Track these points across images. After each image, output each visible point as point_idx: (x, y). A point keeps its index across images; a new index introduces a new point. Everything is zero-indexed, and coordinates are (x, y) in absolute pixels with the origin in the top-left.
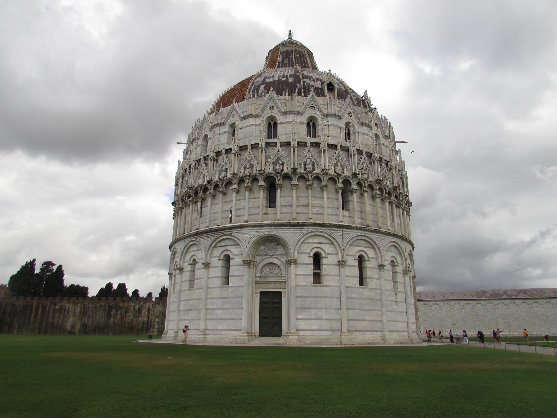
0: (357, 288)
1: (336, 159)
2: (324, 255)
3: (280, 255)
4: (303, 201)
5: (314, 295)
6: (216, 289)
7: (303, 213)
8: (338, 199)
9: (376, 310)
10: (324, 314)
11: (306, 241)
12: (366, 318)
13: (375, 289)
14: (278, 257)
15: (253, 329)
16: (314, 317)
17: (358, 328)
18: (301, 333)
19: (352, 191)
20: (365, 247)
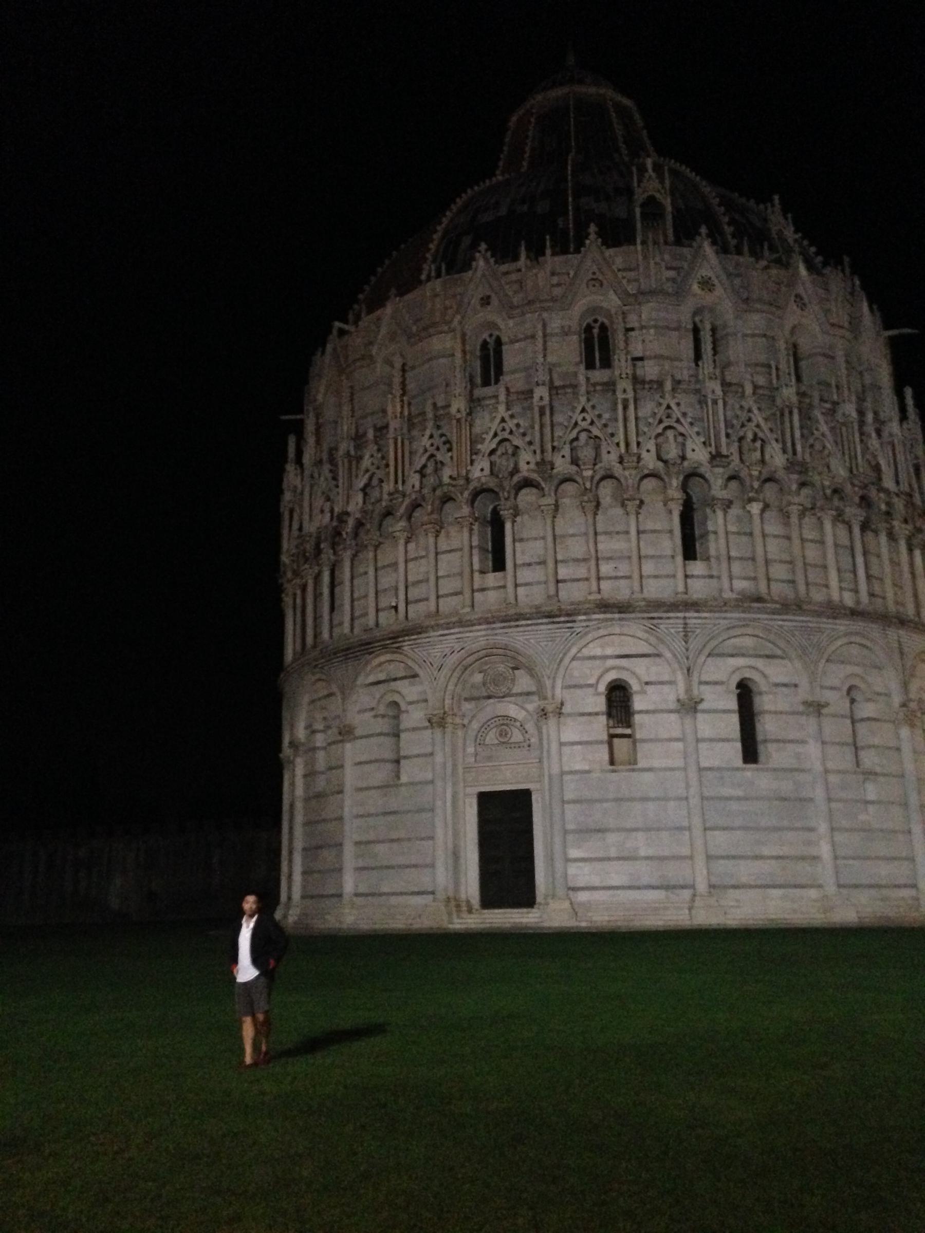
0: (737, 769)
1: (661, 421)
2: (635, 686)
3: (521, 694)
4: (577, 548)
5: (611, 796)
6: (373, 791)
7: (578, 580)
8: (671, 532)
9: (797, 829)
10: (641, 844)
11: (585, 652)
12: (766, 852)
13: (796, 770)
14: (520, 699)
15: (463, 888)
16: (613, 853)
17: (744, 880)
18: (583, 897)
19: (711, 503)
20: (760, 656)
